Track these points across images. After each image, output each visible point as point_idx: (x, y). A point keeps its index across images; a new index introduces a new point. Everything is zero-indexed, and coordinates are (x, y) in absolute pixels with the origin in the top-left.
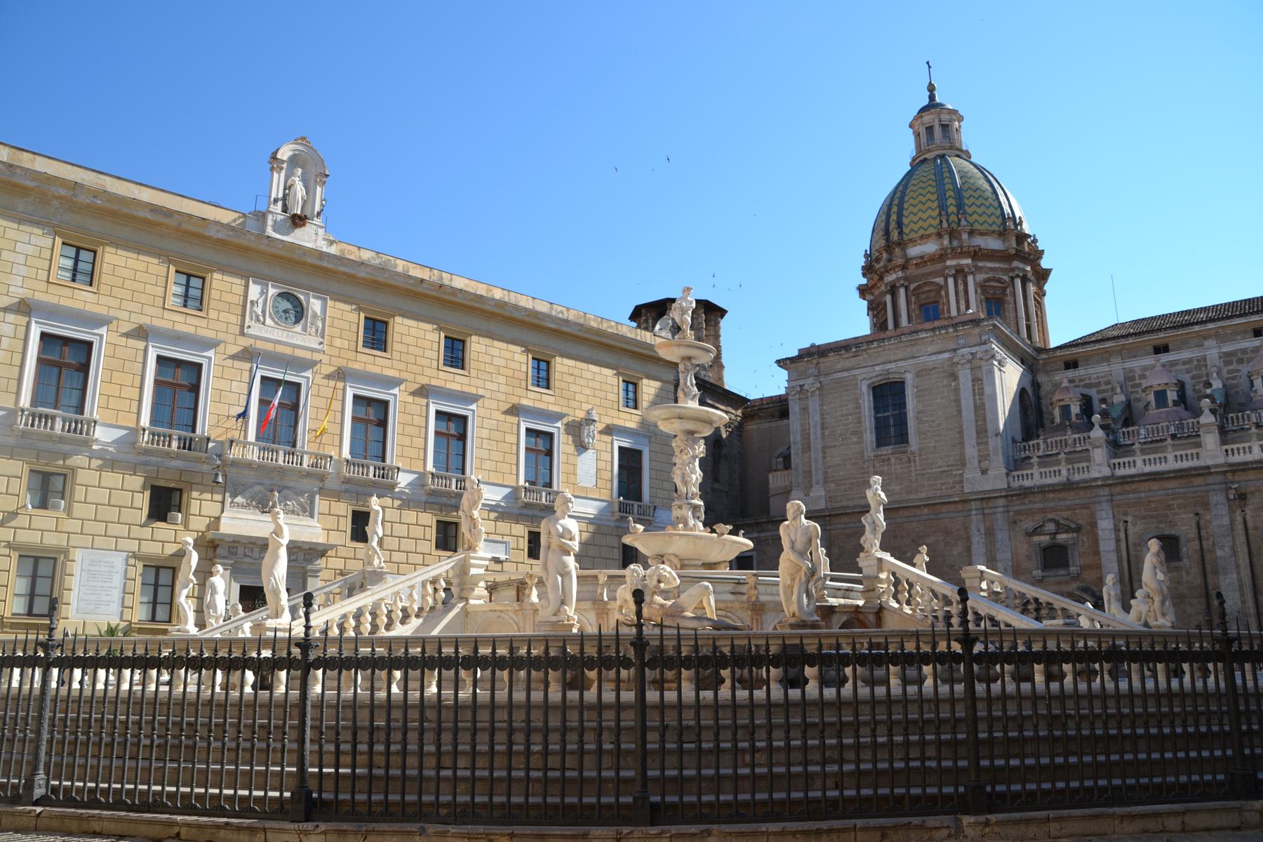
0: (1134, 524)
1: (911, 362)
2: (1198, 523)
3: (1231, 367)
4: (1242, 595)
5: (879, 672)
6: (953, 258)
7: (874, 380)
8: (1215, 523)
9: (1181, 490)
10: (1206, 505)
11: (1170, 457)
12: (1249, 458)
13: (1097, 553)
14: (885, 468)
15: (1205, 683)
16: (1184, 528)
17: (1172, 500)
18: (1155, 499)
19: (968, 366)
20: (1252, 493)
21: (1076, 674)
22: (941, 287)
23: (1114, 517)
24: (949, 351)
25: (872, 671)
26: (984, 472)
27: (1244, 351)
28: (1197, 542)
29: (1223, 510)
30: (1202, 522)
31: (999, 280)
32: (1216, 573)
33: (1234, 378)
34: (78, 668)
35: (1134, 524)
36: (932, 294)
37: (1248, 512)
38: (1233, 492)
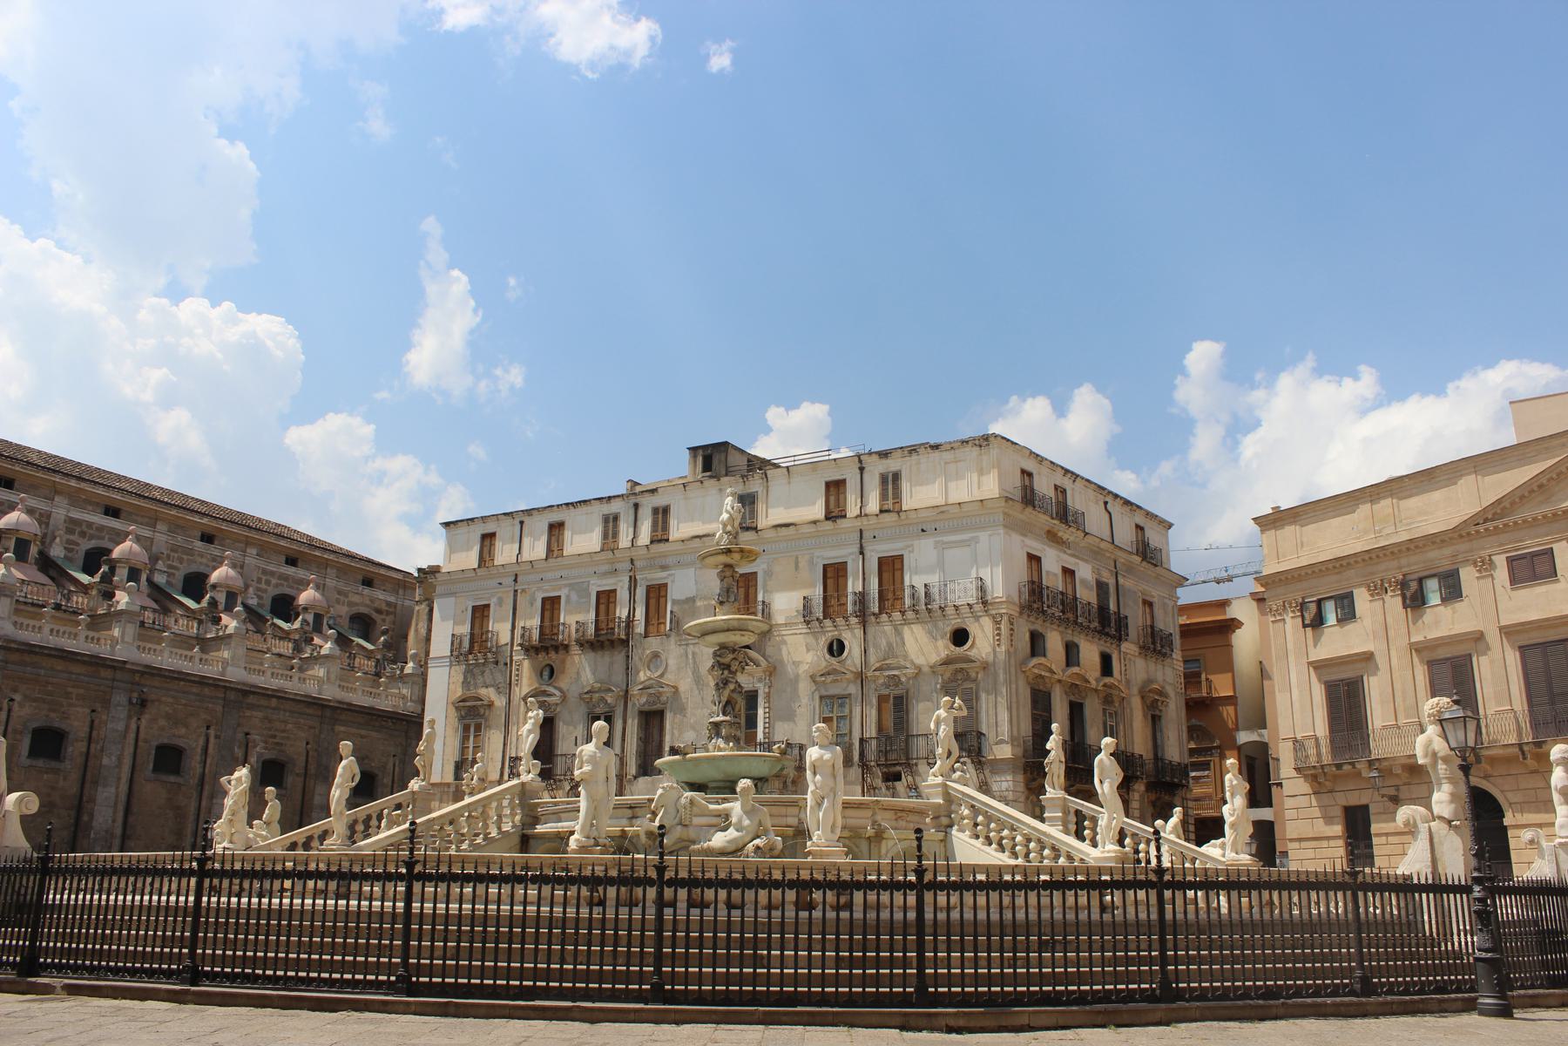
0: (21, 705)
2: (92, 721)
3: (72, 537)
4: (115, 812)
8: (110, 725)
9: (86, 679)
10: (106, 703)
16: (76, 723)
17: (73, 687)
18: (55, 680)
20: (153, 701)
27: (90, 525)
28: (85, 743)
29: (123, 715)
30: (96, 722)
32: (95, 783)
34: (1141, 889)
35: (21, 705)
37: (144, 722)
38: (135, 695)
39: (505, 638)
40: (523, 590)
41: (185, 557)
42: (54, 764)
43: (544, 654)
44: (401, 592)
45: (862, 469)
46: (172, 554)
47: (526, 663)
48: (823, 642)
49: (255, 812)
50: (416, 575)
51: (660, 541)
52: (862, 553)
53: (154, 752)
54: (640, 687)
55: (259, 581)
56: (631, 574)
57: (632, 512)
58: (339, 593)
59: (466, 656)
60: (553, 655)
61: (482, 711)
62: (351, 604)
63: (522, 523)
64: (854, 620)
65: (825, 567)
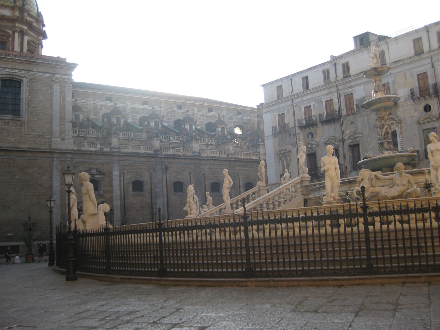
1: (28, 73)
2: (151, 177)
3: (134, 114)
5: (354, 221)
6: (20, 23)
7: (4, 76)
9: (146, 162)
11: (142, 148)
12: (169, 153)
13: (111, 185)
14: (6, 127)
15: (235, 237)
17: (142, 166)
19: (59, 84)
21: (346, 225)
22: (8, 36)
23: (120, 170)
24: (50, 73)
25: (319, 222)
26: (63, 139)
27: (139, 109)
28: (150, 185)
30: (152, 176)
31: (34, 43)
33: (134, 119)
36: (4, 38)
37: (167, 174)
38: (163, 166)
39: (292, 125)
40: (296, 106)
41: (173, 115)
42: (141, 193)
43: (308, 129)
44: (252, 115)
45: (428, 32)
46: (168, 115)
47: (301, 134)
48: (421, 108)
49: (204, 201)
50: (256, 108)
51: (347, 77)
52: (433, 67)
53: (173, 185)
54: (348, 136)
55: (200, 119)
56: (338, 92)
57: (334, 67)
58: (229, 119)
59: (278, 134)
60: (311, 129)
61: (287, 154)
62: (234, 122)
63: (291, 80)
64: (433, 96)
65: (418, 75)
